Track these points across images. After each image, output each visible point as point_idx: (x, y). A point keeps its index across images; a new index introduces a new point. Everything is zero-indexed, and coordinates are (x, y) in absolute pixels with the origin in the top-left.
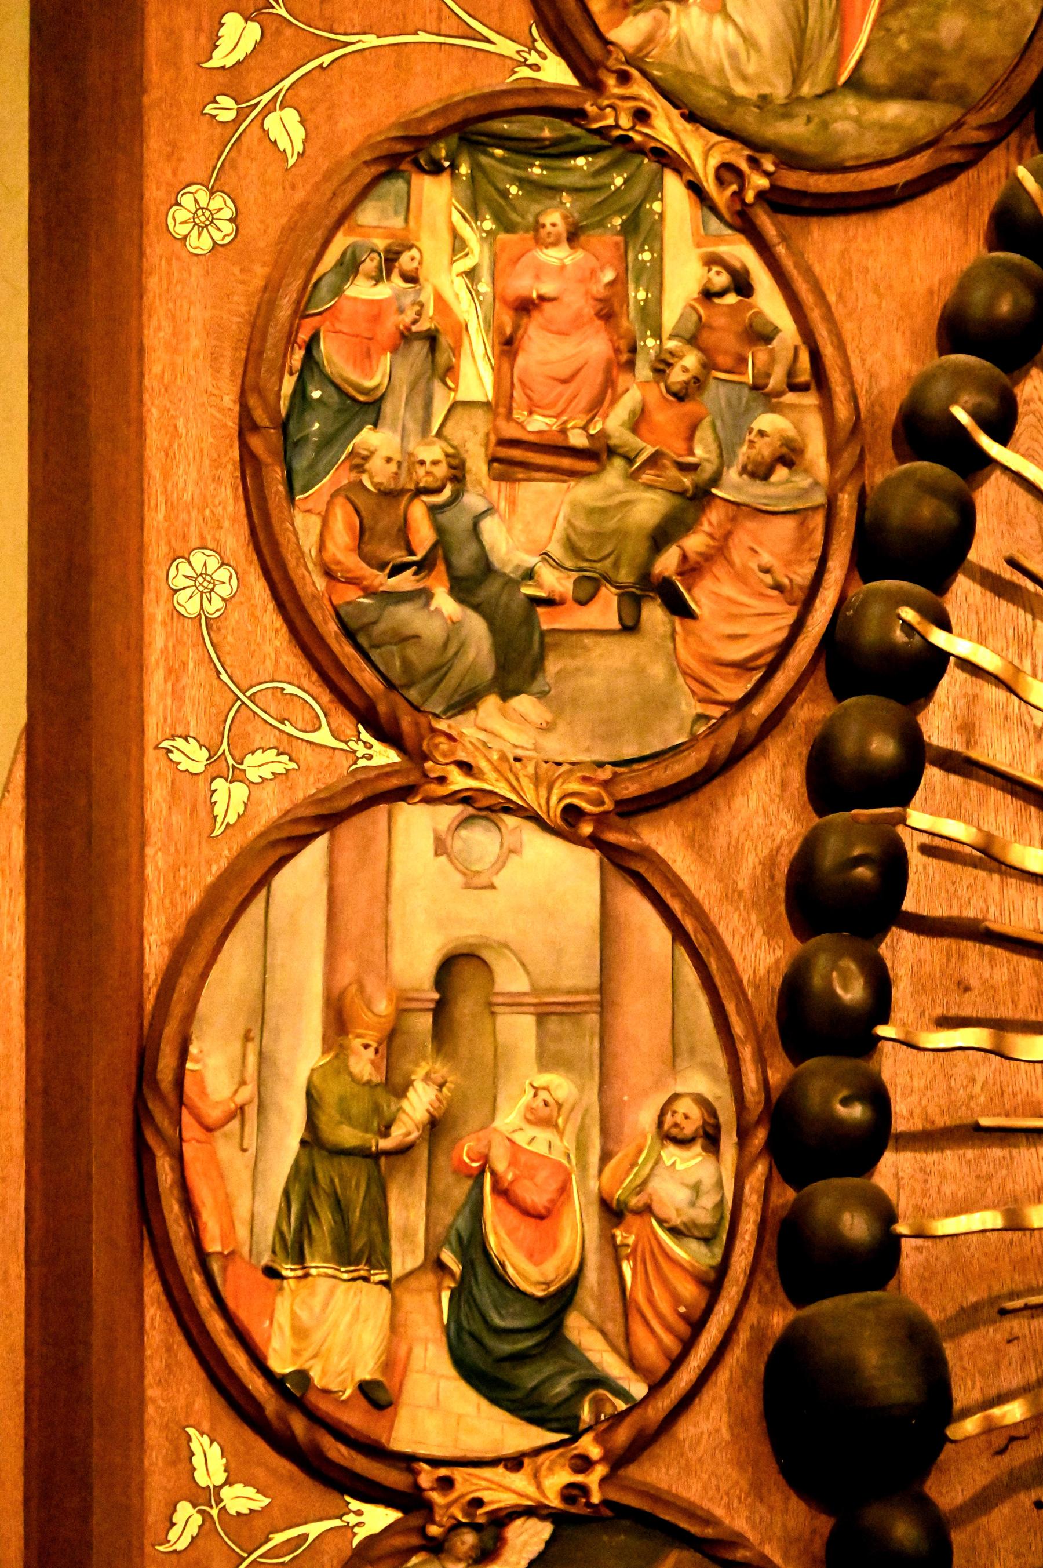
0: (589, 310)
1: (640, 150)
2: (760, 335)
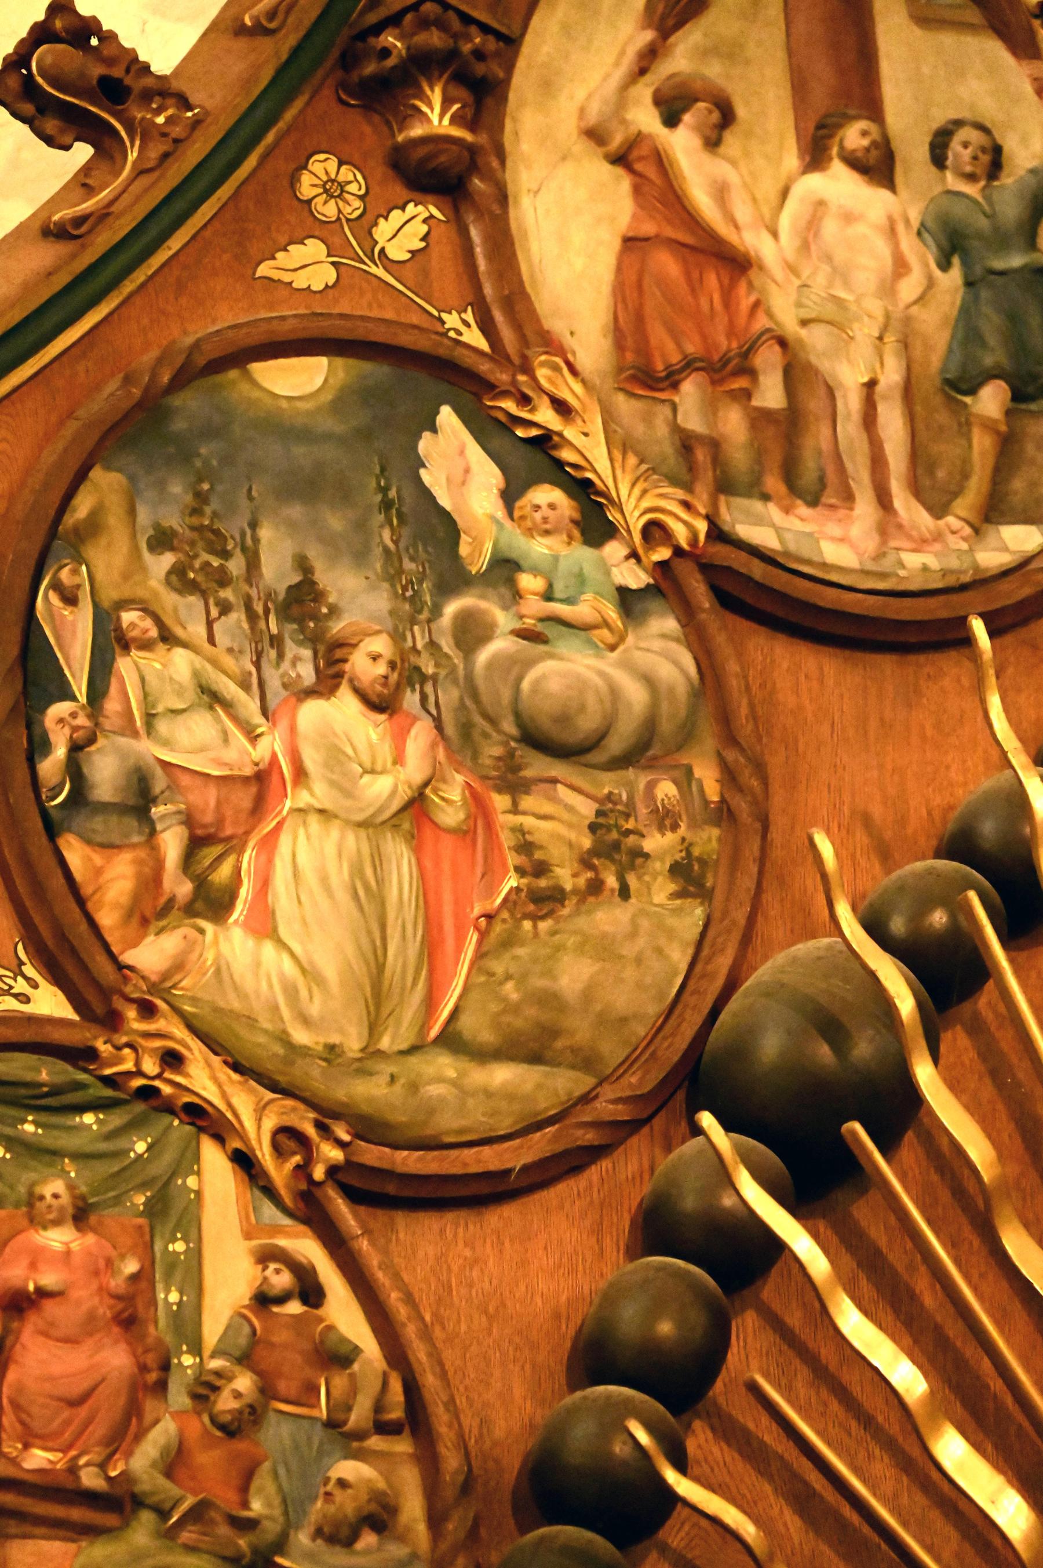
0: (105, 1311)
1: (168, 1108)
2: (338, 1357)
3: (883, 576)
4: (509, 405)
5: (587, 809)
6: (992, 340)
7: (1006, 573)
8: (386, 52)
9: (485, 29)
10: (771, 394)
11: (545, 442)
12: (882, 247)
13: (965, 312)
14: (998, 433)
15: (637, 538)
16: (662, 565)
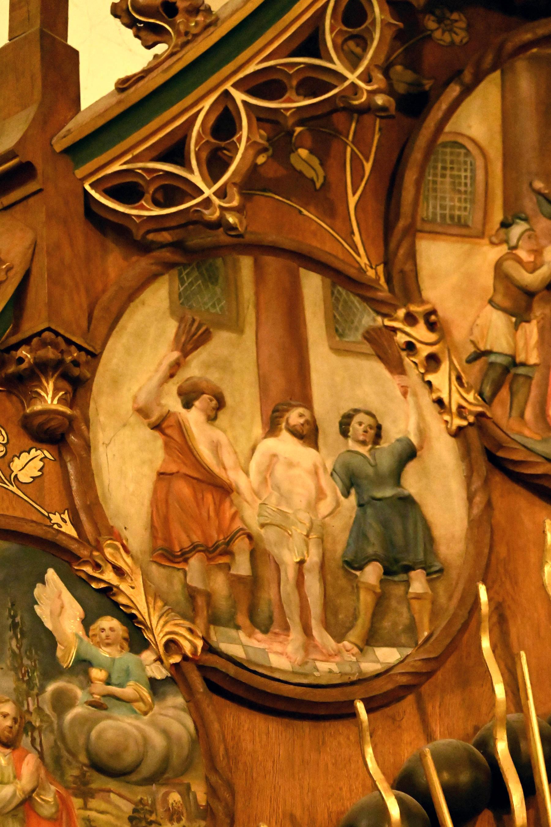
3: (305, 675)
4: (88, 569)
5: (127, 808)
6: (372, 537)
7: (378, 675)
8: (21, 360)
9: (80, 348)
10: (242, 567)
11: (108, 591)
12: (310, 483)
13: (357, 521)
14: (374, 592)
15: (161, 649)
16: (176, 666)
